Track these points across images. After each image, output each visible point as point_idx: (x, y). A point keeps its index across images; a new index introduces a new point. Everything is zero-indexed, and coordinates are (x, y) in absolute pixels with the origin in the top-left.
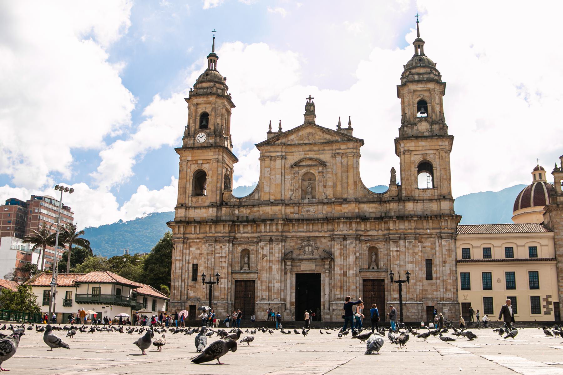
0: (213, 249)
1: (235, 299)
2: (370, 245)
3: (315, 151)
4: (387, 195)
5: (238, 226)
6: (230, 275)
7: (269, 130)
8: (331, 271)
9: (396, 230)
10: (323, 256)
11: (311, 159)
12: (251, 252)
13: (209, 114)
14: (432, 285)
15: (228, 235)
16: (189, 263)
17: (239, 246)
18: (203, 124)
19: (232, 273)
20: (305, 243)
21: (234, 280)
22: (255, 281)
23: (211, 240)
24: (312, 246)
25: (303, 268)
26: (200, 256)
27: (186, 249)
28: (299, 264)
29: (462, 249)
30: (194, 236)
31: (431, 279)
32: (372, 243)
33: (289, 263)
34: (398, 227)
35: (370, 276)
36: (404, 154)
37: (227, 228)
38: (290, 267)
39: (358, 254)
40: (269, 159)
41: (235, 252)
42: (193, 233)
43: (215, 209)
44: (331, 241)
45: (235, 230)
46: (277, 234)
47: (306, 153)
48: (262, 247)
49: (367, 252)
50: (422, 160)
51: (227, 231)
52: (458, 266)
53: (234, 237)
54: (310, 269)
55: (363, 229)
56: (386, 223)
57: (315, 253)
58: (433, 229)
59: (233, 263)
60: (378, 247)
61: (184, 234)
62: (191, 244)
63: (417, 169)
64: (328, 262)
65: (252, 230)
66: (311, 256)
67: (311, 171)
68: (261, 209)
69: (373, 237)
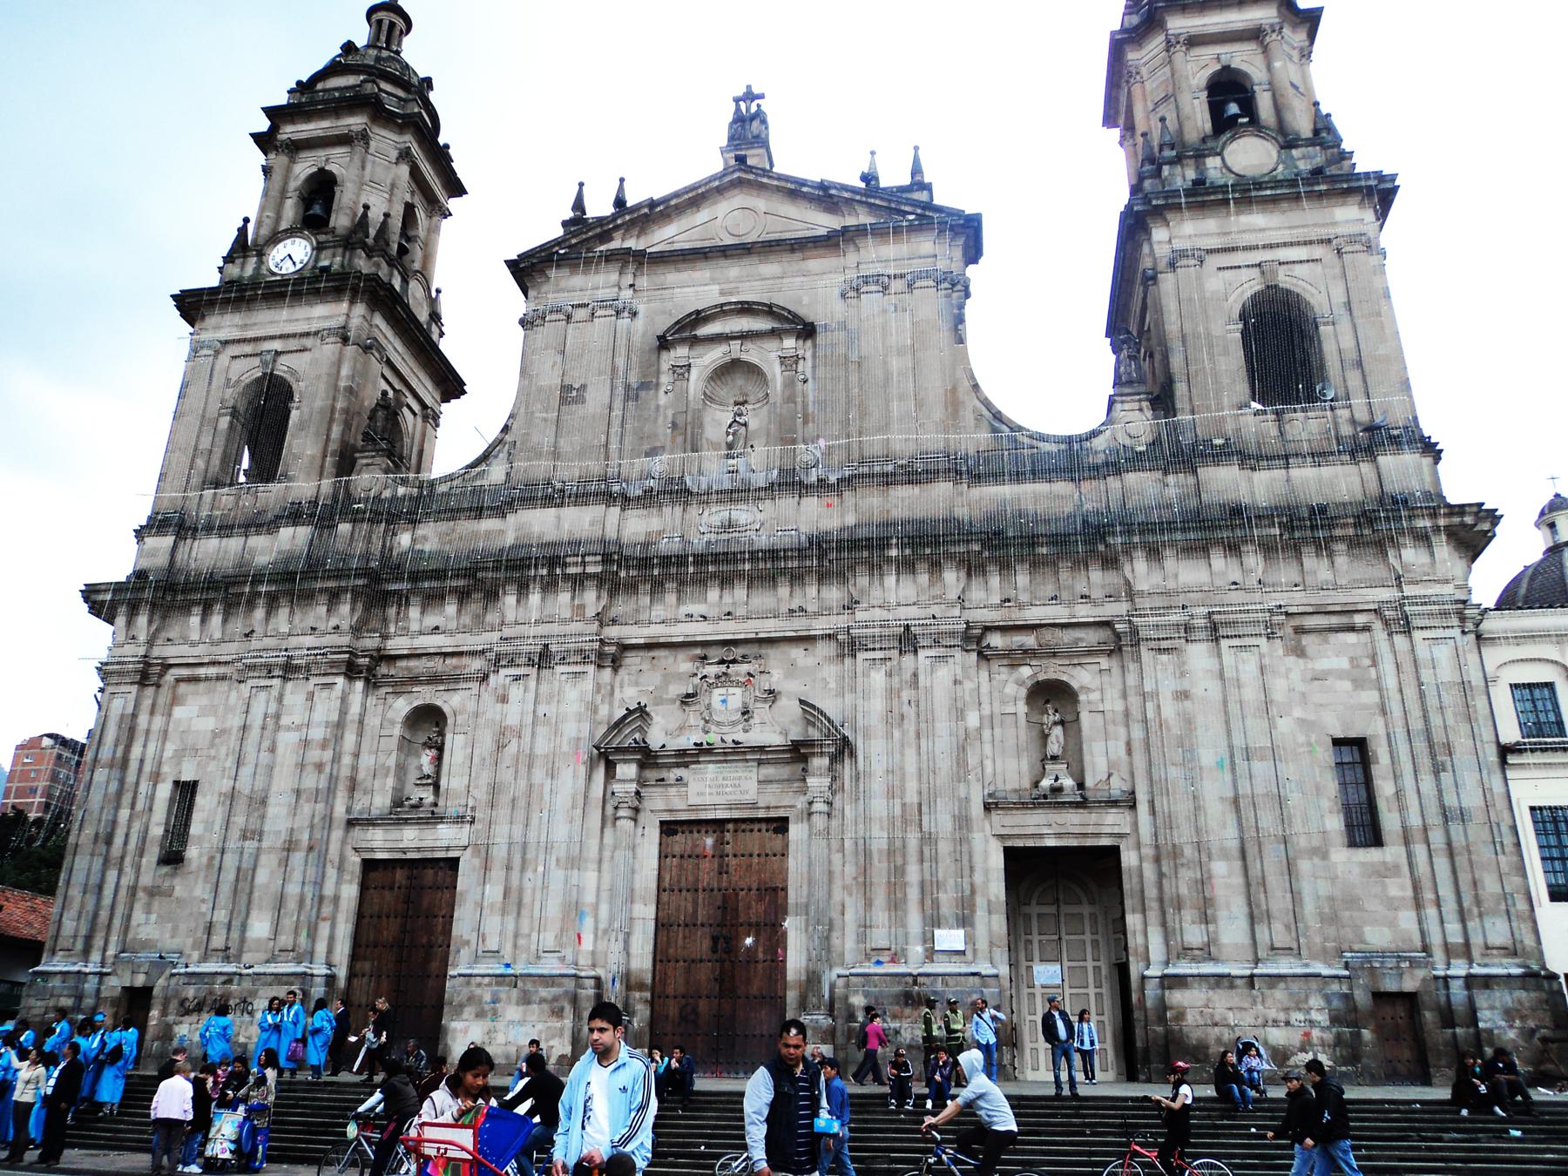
1: (354, 957)
4: (1099, 443)
5: (403, 600)
6: (337, 834)
8: (837, 803)
11: (746, 309)
12: (450, 721)
14: (1385, 872)
15: (345, 640)
16: (156, 777)
17: (398, 694)
19: (351, 823)
20: (712, 670)
21: (355, 860)
22: (457, 859)
26: (212, 745)
27: (152, 713)
29: (1515, 687)
31: (1376, 840)
33: (627, 770)
36: (1172, 265)
37: (345, 609)
38: (633, 787)
42: (195, 636)
45: (385, 620)
47: (723, 286)
48: (500, 691)
49: (1022, 708)
50: (1258, 288)
51: (345, 625)
52: (1510, 774)
53: (379, 650)
54: (732, 798)
56: (1110, 562)
57: (756, 720)
58: (1355, 585)
59: (361, 776)
60: (1075, 684)
61: (150, 643)
62: (183, 687)
64: (826, 761)
67: (744, 357)
68: (511, 518)
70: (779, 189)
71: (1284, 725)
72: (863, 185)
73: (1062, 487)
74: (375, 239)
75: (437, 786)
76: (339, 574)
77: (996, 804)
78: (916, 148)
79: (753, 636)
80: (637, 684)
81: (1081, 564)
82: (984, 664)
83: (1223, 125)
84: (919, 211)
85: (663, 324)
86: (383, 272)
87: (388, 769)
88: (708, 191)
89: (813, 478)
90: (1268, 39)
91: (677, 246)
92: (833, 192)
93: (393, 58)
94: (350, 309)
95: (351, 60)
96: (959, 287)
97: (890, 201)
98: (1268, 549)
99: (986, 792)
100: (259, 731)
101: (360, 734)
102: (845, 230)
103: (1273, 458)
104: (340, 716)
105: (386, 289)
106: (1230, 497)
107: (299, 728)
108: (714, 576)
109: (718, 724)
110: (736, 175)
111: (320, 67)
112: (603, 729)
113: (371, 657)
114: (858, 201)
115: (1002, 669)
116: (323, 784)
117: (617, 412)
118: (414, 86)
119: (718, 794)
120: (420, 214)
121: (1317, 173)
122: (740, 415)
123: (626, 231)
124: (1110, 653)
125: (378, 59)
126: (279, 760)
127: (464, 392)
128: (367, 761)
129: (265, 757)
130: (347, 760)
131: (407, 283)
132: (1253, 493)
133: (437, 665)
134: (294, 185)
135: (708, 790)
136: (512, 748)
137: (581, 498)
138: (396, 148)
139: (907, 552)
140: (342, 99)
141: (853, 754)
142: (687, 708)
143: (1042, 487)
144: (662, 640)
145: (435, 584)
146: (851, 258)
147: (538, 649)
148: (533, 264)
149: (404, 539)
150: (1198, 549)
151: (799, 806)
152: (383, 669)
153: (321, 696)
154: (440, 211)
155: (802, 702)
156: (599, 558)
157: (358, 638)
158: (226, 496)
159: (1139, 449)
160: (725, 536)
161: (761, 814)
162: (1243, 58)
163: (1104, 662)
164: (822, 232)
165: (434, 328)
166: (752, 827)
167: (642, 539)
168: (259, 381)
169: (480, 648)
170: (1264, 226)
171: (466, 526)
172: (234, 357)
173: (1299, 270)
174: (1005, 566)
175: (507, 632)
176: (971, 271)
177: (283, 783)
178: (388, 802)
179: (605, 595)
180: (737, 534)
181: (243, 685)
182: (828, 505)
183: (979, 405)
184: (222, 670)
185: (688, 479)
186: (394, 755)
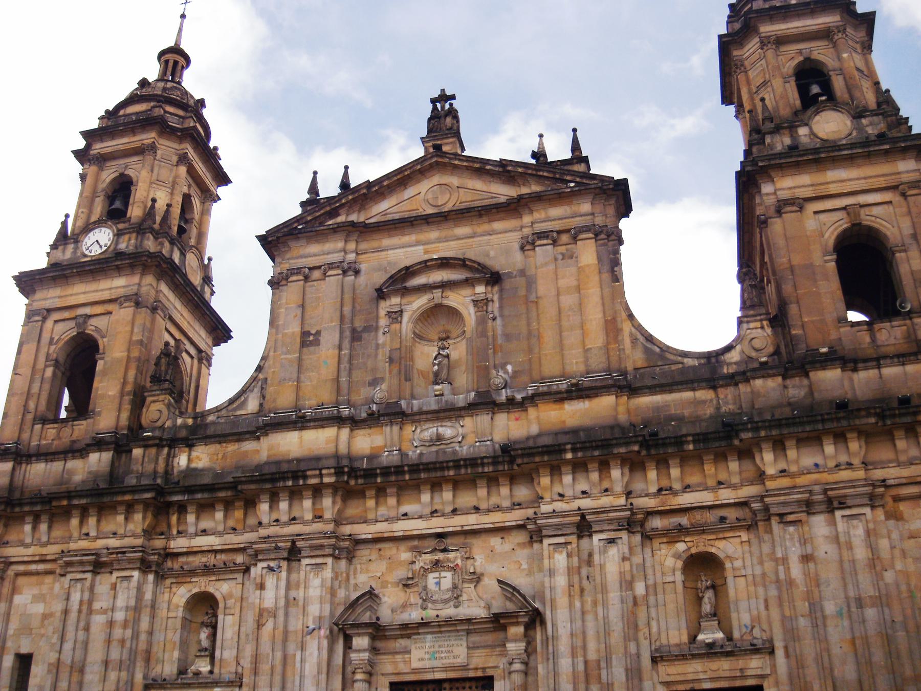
0: (86, 596)
2: (689, 548)
3: (462, 239)
5: (182, 509)
7: (308, 196)
8: (532, 664)
9: (792, 476)
10: (499, 606)
11: (444, 263)
12: (221, 605)
13: (134, 180)
15: (139, 541)
18: (113, 207)
20: (428, 557)
23: (81, 563)
24: (454, 569)
25: (422, 659)
26: (42, 625)
28: (403, 642)
30: (30, 551)
32: (695, 538)
33: (361, 642)
34: (797, 462)
35: (702, 676)
36: (779, 212)
38: (366, 655)
39: (640, 588)
40: (301, 277)
41: (165, 605)
42: (28, 540)
43: (107, 456)
44: (531, 541)
45: (169, 526)
46: (318, 527)
47: (426, 247)
48: (259, 581)
49: (679, 577)
51: (139, 530)
53: (165, 549)
55: (653, 489)
56: (746, 453)
57: (464, 597)
59: (156, 649)
60: (721, 555)
62: (21, 581)
63: (835, 257)
64: (521, 629)
65: (231, 523)
66: (449, 611)
67: (446, 302)
69: (698, 517)
70: (467, 168)
71: (889, 576)
72: (533, 162)
73: (704, 394)
74: (160, 225)
75: (212, 657)
76: (134, 490)
77: (662, 657)
78: (575, 130)
79: (459, 529)
80: (368, 571)
81: (721, 457)
82: (648, 542)
83: (809, 103)
84: (578, 180)
85: (379, 279)
86: (166, 249)
87: (175, 643)
88: (411, 173)
89: (503, 396)
90: (836, 37)
91: (389, 217)
92: (510, 168)
93: (176, 88)
94: (141, 279)
95: (145, 91)
96: (613, 237)
97: (554, 173)
98: (867, 435)
99: (653, 648)
100: (77, 614)
101: (153, 616)
102: (520, 198)
103: (865, 361)
104: (136, 602)
105: (168, 263)
106: (837, 394)
107: (104, 612)
108: (425, 481)
109: (434, 602)
110: (434, 160)
111: (122, 97)
112: (341, 609)
113: (159, 554)
114: (530, 174)
115: (663, 546)
116: (125, 656)
117: (345, 352)
118: (191, 107)
119: (436, 659)
120: (196, 202)
121: (881, 137)
122: (443, 349)
123: (350, 207)
124: (748, 528)
125: (164, 89)
126: (92, 637)
127: (231, 337)
128: (159, 637)
129: (81, 633)
130: (143, 637)
131: (185, 256)
132: (853, 389)
133: (210, 560)
134: (102, 186)
135: (427, 656)
136: (269, 626)
137: (321, 421)
138: (177, 154)
139: (580, 454)
140: (138, 121)
141: (543, 623)
142: (408, 590)
143: (688, 395)
144: (386, 535)
145: (206, 495)
146: (527, 219)
147: (289, 544)
148: (278, 238)
149: (182, 460)
150: (813, 440)
151: (502, 666)
152: (169, 564)
153: (122, 586)
154: (210, 197)
155: (499, 581)
156: (332, 471)
157: (149, 540)
158: (51, 431)
159: (763, 359)
160: (434, 449)
161: (471, 674)
162: (820, 52)
163: (744, 536)
164: (503, 199)
165: (207, 289)
166: (463, 685)
167: (367, 452)
168: (73, 338)
169: (242, 546)
170: (846, 178)
171: (231, 448)
172: (56, 322)
173: (876, 211)
174: (662, 464)
175: (263, 532)
176: (624, 224)
177: (96, 655)
178: (175, 671)
179: (339, 500)
180: (442, 447)
181: (63, 579)
182: (517, 419)
183: (633, 330)
184: (48, 566)
185: (403, 403)
186: (179, 631)
